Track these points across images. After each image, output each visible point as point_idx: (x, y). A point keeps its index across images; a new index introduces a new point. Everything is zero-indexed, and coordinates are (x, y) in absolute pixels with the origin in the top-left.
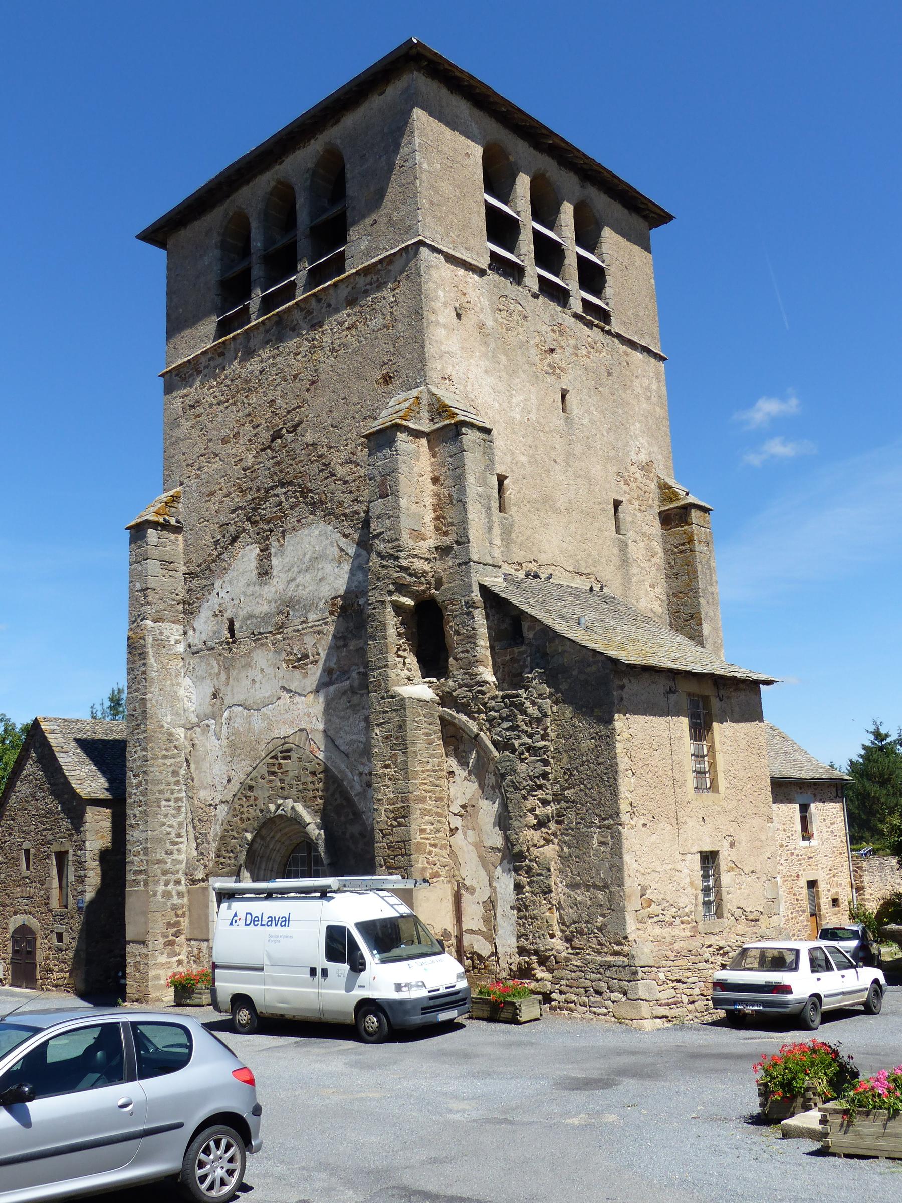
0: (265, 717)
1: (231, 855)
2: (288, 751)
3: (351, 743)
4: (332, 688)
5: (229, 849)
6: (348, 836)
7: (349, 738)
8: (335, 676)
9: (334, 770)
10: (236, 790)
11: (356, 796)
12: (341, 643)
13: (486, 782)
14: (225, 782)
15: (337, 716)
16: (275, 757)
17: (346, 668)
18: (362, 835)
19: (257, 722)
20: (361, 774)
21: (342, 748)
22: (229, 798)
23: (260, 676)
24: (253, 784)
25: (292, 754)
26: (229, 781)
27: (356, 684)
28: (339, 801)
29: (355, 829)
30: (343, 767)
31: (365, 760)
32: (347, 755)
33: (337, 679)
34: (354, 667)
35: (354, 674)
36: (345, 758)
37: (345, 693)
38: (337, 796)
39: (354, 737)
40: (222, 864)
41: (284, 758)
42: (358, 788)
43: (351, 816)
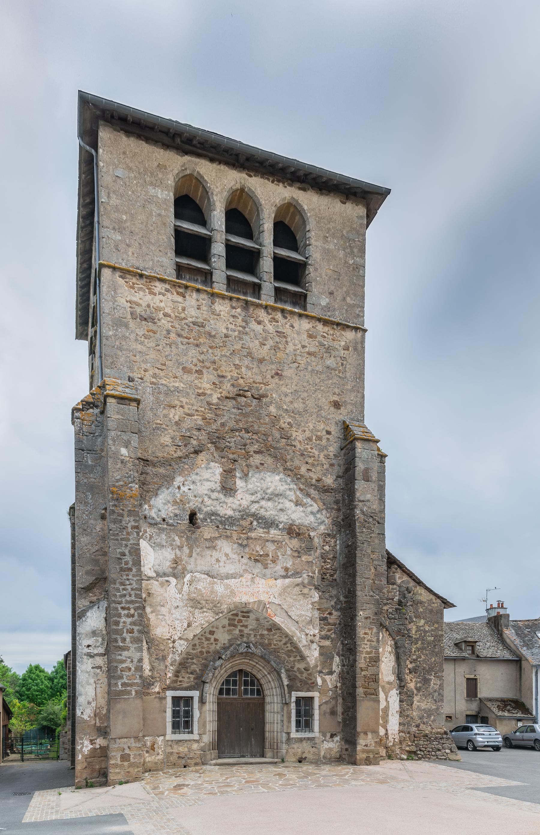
0: (227, 586)
1: (191, 676)
2: (248, 612)
3: (300, 616)
4: (287, 581)
5: (189, 671)
6: (295, 669)
7: (299, 612)
8: (290, 573)
9: (286, 630)
10: (198, 632)
11: (303, 646)
12: (296, 554)
13: (386, 650)
14: (185, 625)
15: (291, 597)
16: (237, 615)
17: (298, 570)
18: (306, 669)
19: (220, 588)
20: (307, 635)
21: (293, 618)
22: (191, 636)
23: (224, 558)
24: (214, 629)
25: (251, 615)
26: (189, 625)
27: (306, 581)
28: (289, 648)
29: (302, 666)
30: (293, 629)
31: (311, 627)
32: (297, 622)
33: (291, 575)
34: (305, 571)
35: (305, 575)
36: (296, 624)
37: (298, 585)
38: (289, 645)
39: (303, 613)
40: (180, 681)
41: (244, 617)
42: (304, 642)
43: (298, 658)
